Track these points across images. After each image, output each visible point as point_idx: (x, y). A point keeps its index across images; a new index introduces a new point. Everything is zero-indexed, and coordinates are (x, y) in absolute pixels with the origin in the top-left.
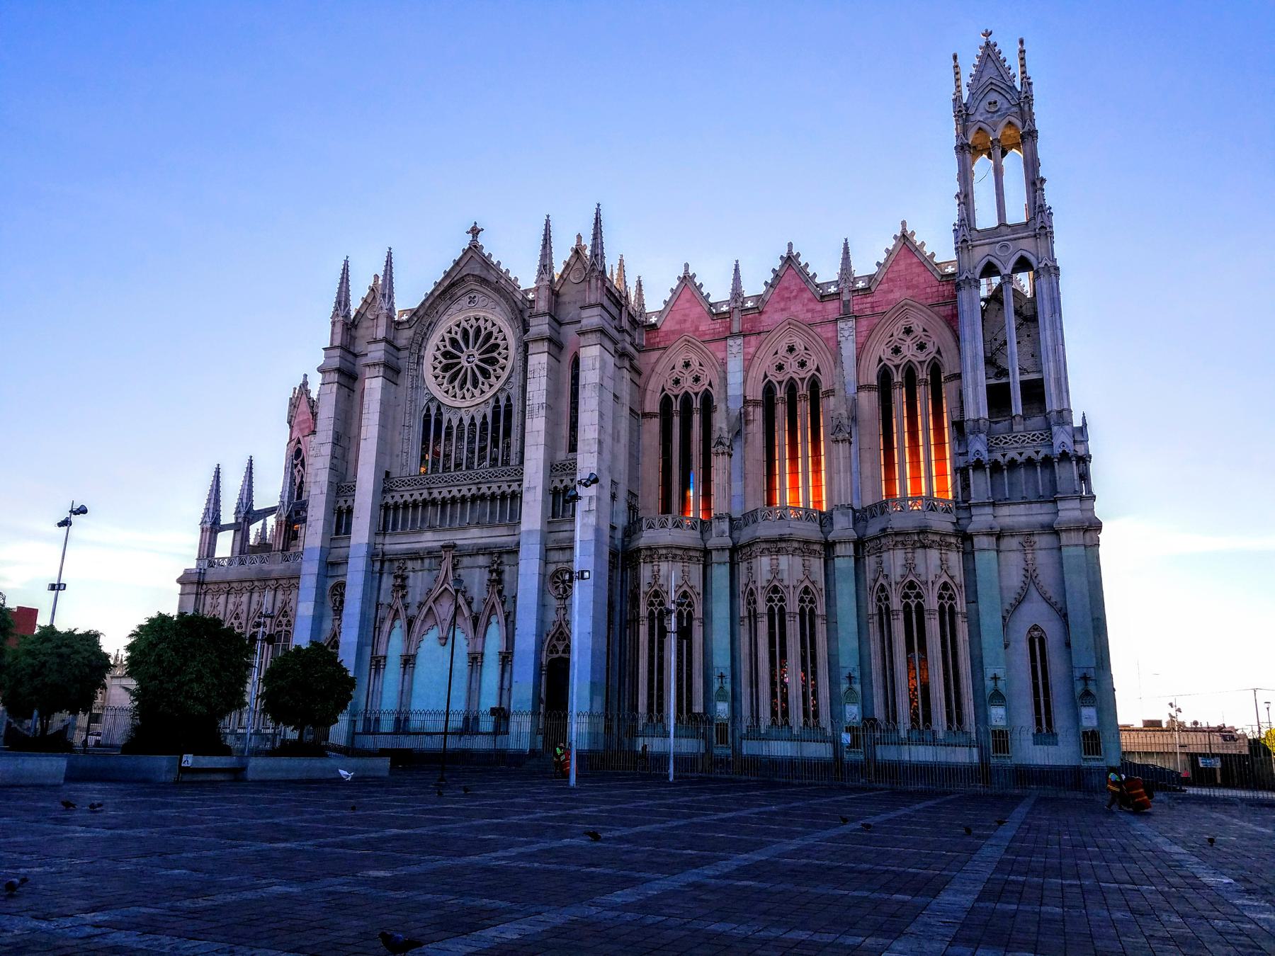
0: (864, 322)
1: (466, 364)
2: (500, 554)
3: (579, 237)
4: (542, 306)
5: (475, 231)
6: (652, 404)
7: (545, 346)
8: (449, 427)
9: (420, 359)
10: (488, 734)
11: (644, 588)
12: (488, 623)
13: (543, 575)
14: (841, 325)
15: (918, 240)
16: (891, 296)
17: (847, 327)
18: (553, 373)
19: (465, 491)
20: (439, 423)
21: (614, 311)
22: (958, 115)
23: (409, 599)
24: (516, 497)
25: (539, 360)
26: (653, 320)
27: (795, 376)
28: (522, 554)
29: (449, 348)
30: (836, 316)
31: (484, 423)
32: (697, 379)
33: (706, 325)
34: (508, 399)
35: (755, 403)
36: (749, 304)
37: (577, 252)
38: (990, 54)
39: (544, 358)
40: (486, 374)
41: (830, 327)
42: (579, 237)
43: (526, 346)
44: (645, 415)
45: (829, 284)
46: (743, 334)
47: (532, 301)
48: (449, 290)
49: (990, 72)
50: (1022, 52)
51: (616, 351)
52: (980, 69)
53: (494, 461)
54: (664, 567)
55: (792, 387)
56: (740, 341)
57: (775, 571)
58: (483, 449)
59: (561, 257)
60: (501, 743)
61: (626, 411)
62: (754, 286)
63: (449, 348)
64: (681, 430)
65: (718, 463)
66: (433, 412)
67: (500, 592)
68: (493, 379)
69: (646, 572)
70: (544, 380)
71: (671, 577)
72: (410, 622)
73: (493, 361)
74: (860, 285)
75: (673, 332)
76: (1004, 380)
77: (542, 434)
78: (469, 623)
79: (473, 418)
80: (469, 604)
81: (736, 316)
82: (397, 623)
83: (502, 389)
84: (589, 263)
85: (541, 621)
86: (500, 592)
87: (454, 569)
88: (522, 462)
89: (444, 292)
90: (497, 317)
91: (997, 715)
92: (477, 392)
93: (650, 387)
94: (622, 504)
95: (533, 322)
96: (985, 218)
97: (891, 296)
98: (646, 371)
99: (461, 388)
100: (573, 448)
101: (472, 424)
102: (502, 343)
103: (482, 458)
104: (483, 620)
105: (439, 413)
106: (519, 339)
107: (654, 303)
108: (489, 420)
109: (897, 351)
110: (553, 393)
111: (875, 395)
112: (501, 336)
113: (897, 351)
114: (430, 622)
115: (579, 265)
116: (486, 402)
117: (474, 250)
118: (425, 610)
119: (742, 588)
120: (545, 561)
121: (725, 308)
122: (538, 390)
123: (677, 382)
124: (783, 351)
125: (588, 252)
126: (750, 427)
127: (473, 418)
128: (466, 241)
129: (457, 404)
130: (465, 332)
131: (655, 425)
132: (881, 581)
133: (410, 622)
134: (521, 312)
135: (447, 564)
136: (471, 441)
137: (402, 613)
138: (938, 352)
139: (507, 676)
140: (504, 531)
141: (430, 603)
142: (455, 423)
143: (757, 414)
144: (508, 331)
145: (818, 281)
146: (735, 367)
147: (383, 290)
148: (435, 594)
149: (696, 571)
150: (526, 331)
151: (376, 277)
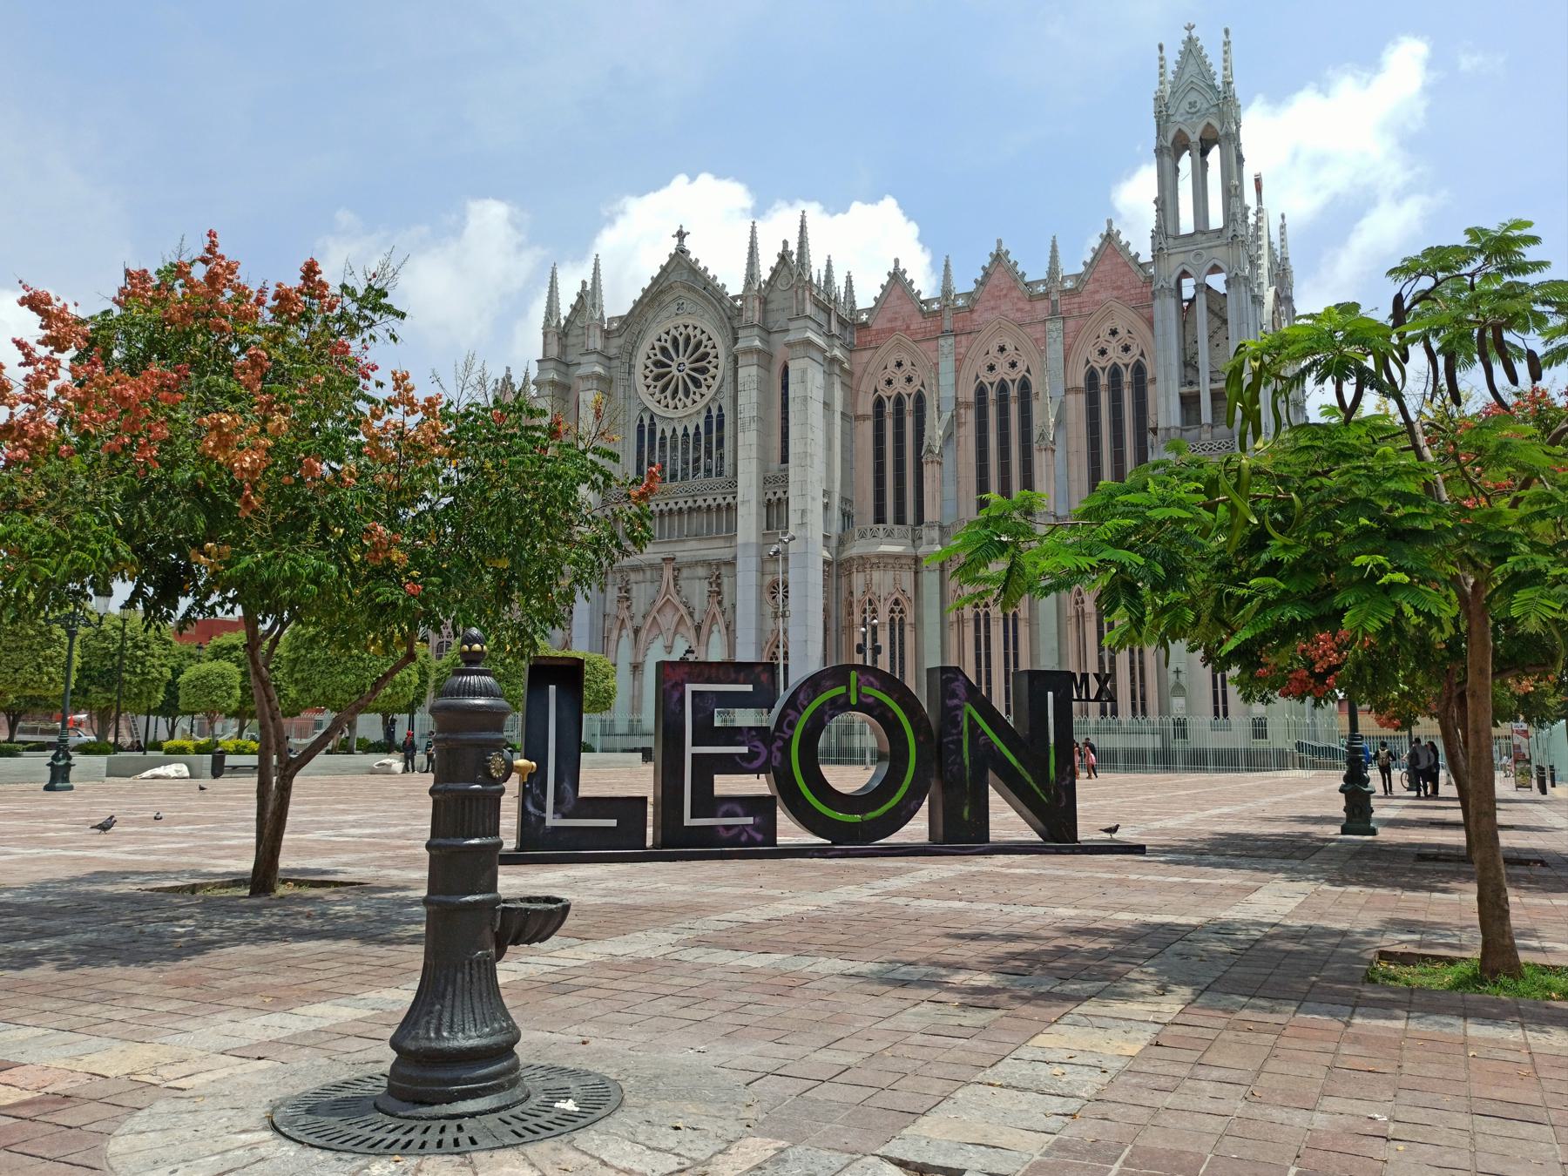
0: (1071, 323)
1: (675, 372)
2: (718, 566)
3: (785, 243)
4: (753, 314)
5: (681, 235)
6: (866, 406)
7: (755, 359)
8: (663, 438)
9: (631, 367)
11: (858, 594)
12: (710, 632)
13: (760, 586)
14: (1049, 325)
15: (1123, 238)
16: (1097, 297)
17: (1055, 327)
18: (763, 386)
19: (681, 504)
20: (652, 433)
21: (822, 318)
22: (1158, 115)
23: (634, 609)
24: (731, 508)
25: (749, 373)
26: (864, 317)
27: (1007, 378)
28: (739, 562)
29: (660, 357)
30: (1044, 316)
31: (697, 433)
32: (909, 380)
33: (917, 323)
34: (720, 409)
35: (967, 405)
36: (960, 302)
37: (784, 257)
38: (1191, 49)
39: (754, 370)
40: (697, 383)
41: (1039, 327)
42: (785, 243)
43: (736, 361)
44: (857, 418)
45: (1038, 282)
46: (955, 334)
47: (740, 309)
48: (654, 296)
49: (1191, 68)
50: (1227, 44)
51: (825, 358)
52: (1181, 66)
53: (708, 471)
54: (877, 576)
55: (1003, 387)
56: (951, 340)
58: (697, 460)
59: (767, 263)
61: (838, 417)
62: (964, 283)
63: (660, 357)
64: (892, 436)
65: (928, 471)
66: (646, 422)
67: (720, 603)
68: (704, 390)
69: (858, 580)
70: (754, 393)
71: (884, 582)
72: (637, 631)
73: (704, 371)
74: (1069, 285)
75: (883, 331)
76: (1195, 389)
77: (754, 448)
80: (691, 615)
81: (948, 314)
82: (624, 632)
83: (713, 399)
84: (791, 266)
85: (760, 630)
86: (720, 603)
87: (676, 578)
88: (736, 474)
89: (652, 300)
90: (706, 325)
91: (1178, 703)
92: (689, 402)
93: (862, 388)
94: (836, 514)
95: (741, 333)
96: (1187, 224)
97: (1097, 297)
98: (858, 371)
99: (673, 398)
100: (785, 459)
101: (686, 434)
102: (713, 352)
103: (696, 469)
104: (705, 630)
105: (652, 424)
106: (728, 348)
107: (865, 298)
108: (702, 430)
109: (1103, 352)
110: (764, 404)
111: (1082, 398)
112: (710, 344)
113: (1103, 352)
114: (655, 631)
115: (785, 272)
116: (698, 412)
117: (681, 254)
118: (650, 620)
119: (951, 593)
120: (762, 573)
121: (936, 306)
122: (749, 401)
123: (889, 382)
124: (994, 350)
125: (794, 257)
126: (962, 430)
128: (671, 246)
129: (670, 413)
130: (675, 341)
131: (868, 428)
133: (637, 631)
134: (729, 313)
135: (668, 573)
136: (685, 452)
137: (629, 624)
138: (1142, 354)
140: (721, 543)
141: (654, 613)
142: (668, 434)
143: (970, 416)
144: (717, 339)
145: (1027, 279)
146: (947, 366)
147: (588, 298)
148: (659, 604)
149: (907, 579)
150: (736, 340)
151: (584, 283)
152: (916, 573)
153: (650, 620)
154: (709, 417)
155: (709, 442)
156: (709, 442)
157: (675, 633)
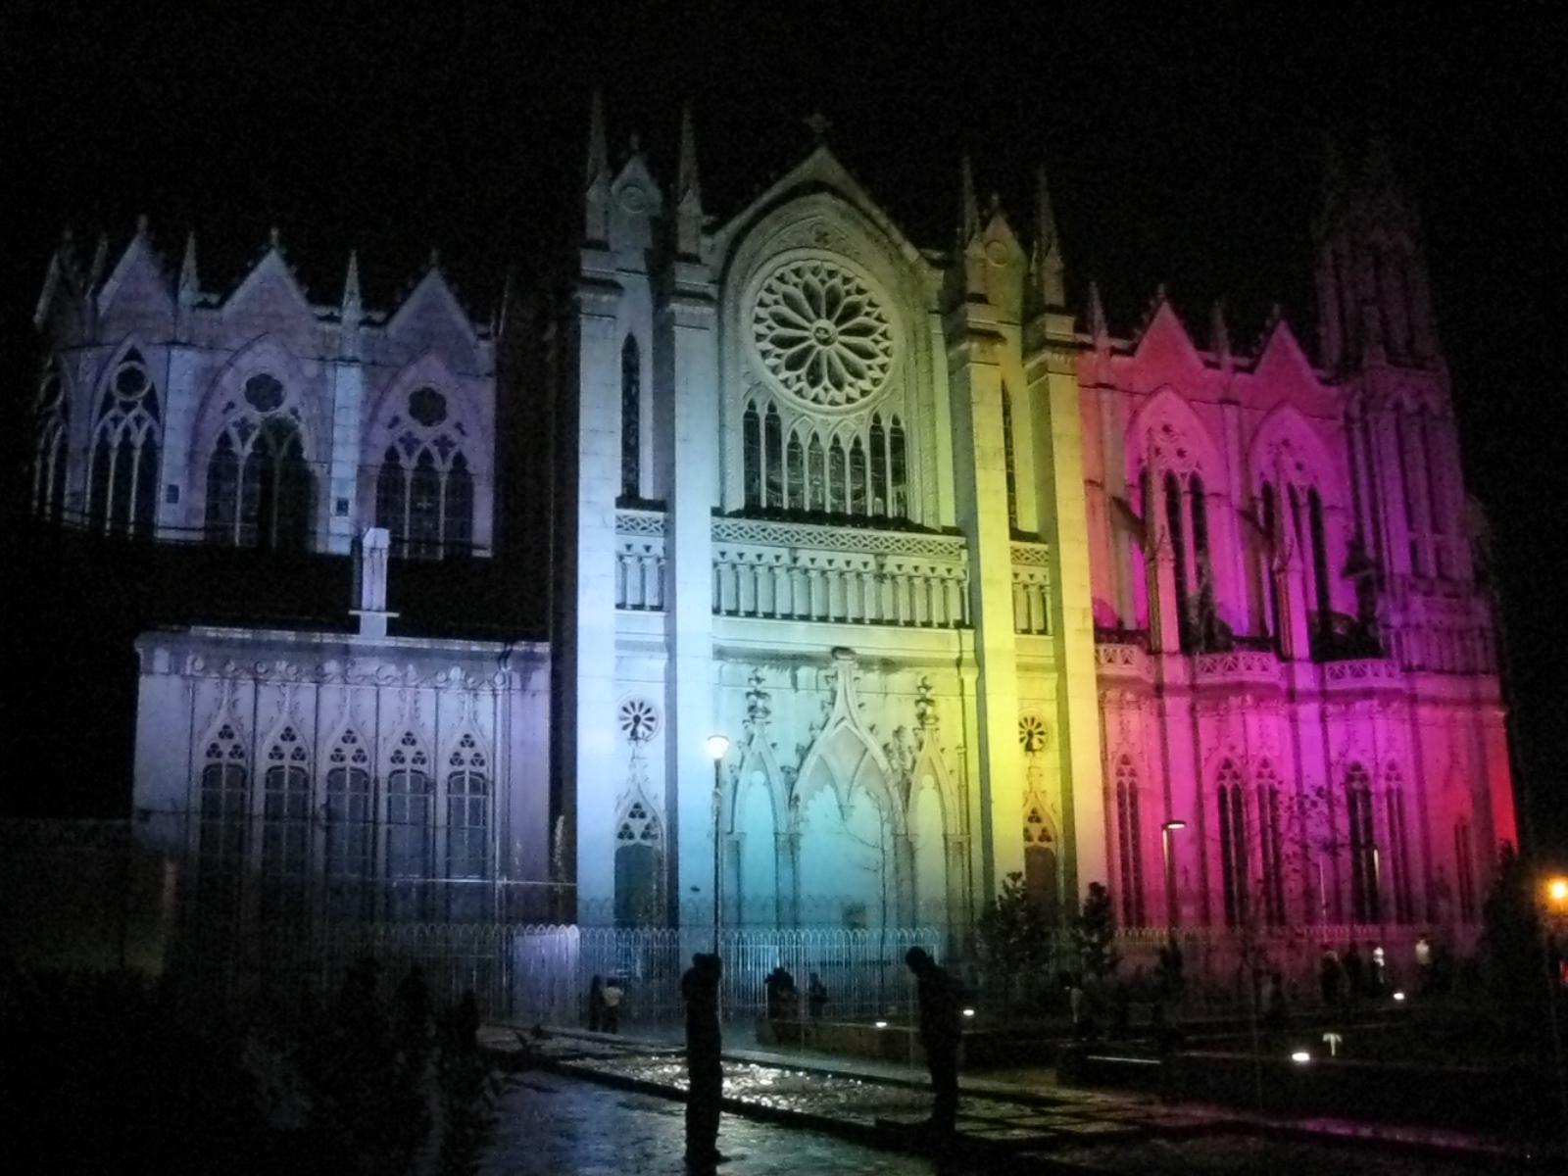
8: (794, 444)
20: (774, 432)
31: (856, 451)
34: (896, 421)
66: (762, 412)
79: (836, 440)
101: (836, 447)
108: (866, 447)
127: (836, 440)
136: (838, 474)
142: (805, 441)
154: (876, 428)
155: (879, 468)
156: (879, 468)
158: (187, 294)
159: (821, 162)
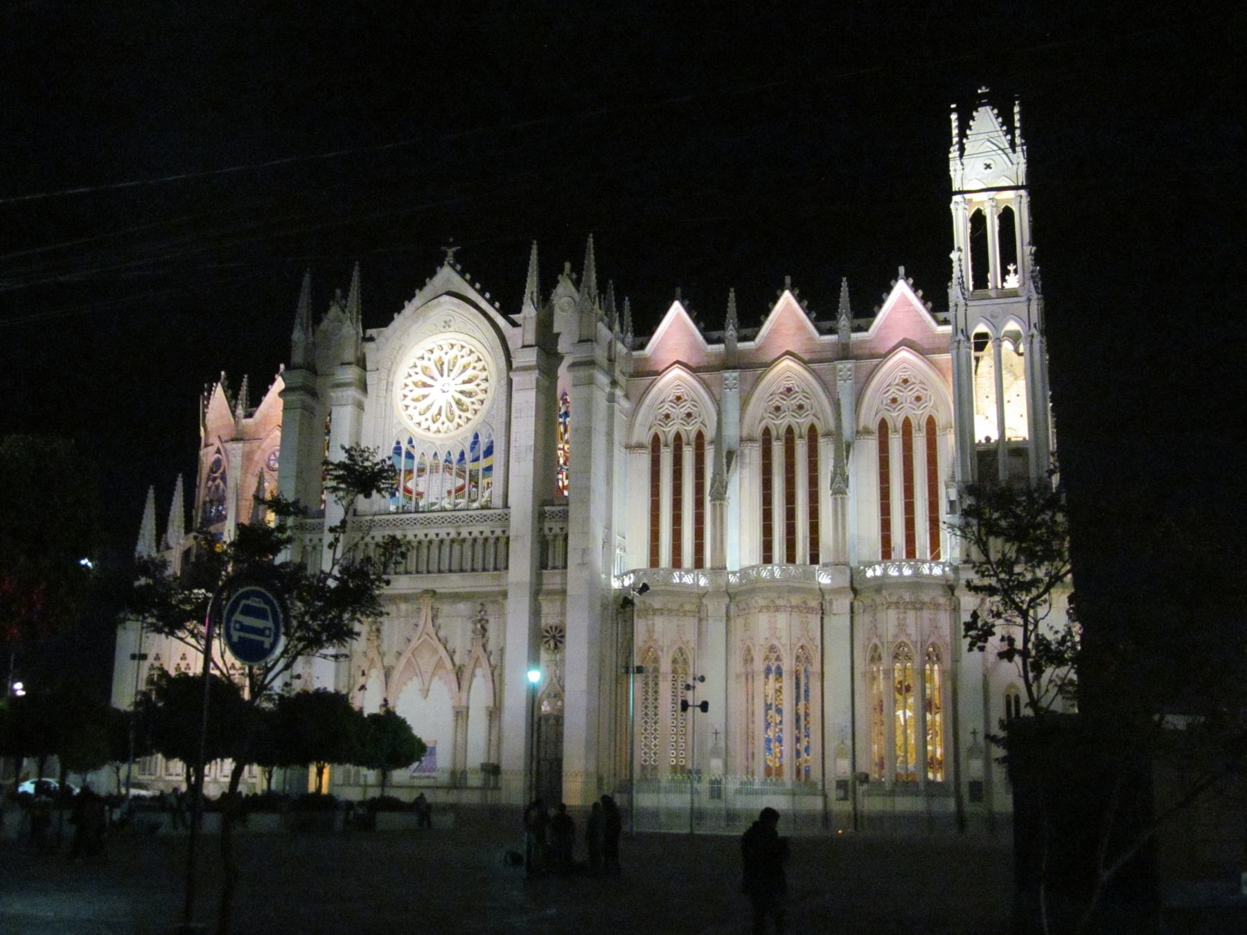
10: (477, 788)
12: (473, 675)
23: (385, 648)
57: (773, 629)
60: (491, 798)
67: (484, 647)
69: (640, 626)
72: (388, 674)
78: (453, 677)
80: (451, 655)
86: (484, 647)
87: (434, 618)
104: (467, 675)
132: (875, 641)
133: (388, 674)
139: (494, 732)
152: (700, 620)
153: (403, 660)
157: (433, 674)
158: (240, 411)
159: (447, 276)
